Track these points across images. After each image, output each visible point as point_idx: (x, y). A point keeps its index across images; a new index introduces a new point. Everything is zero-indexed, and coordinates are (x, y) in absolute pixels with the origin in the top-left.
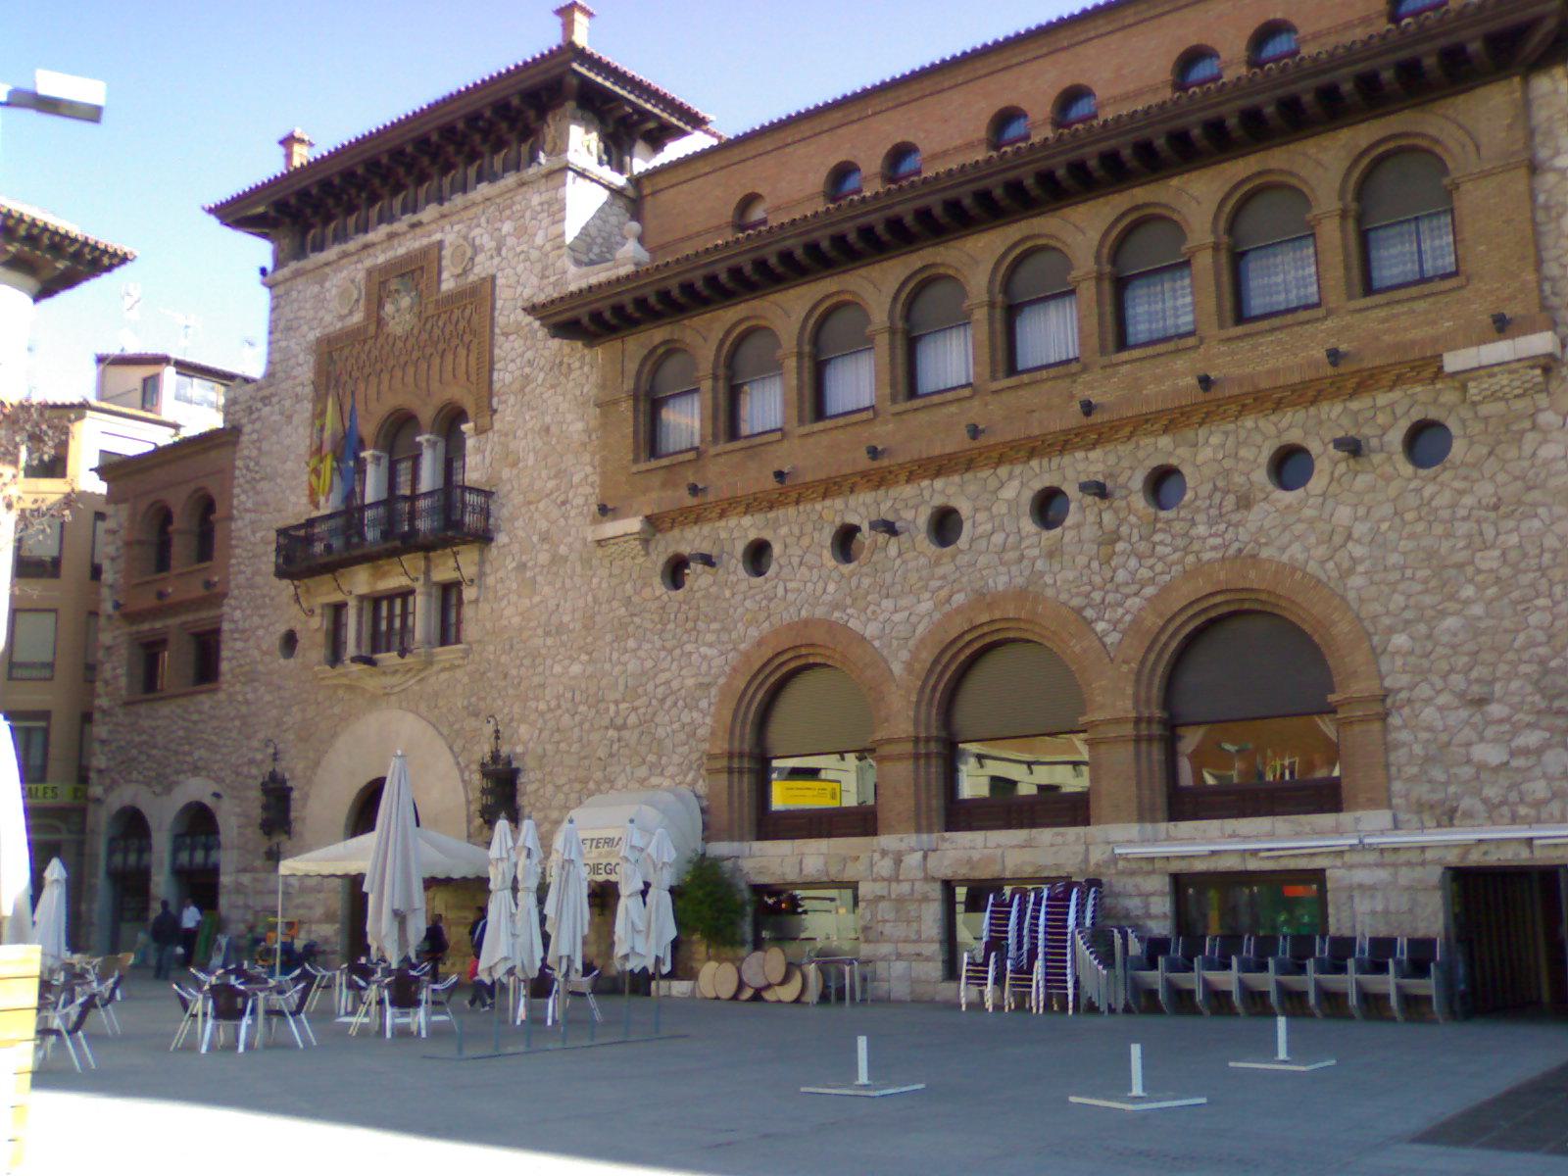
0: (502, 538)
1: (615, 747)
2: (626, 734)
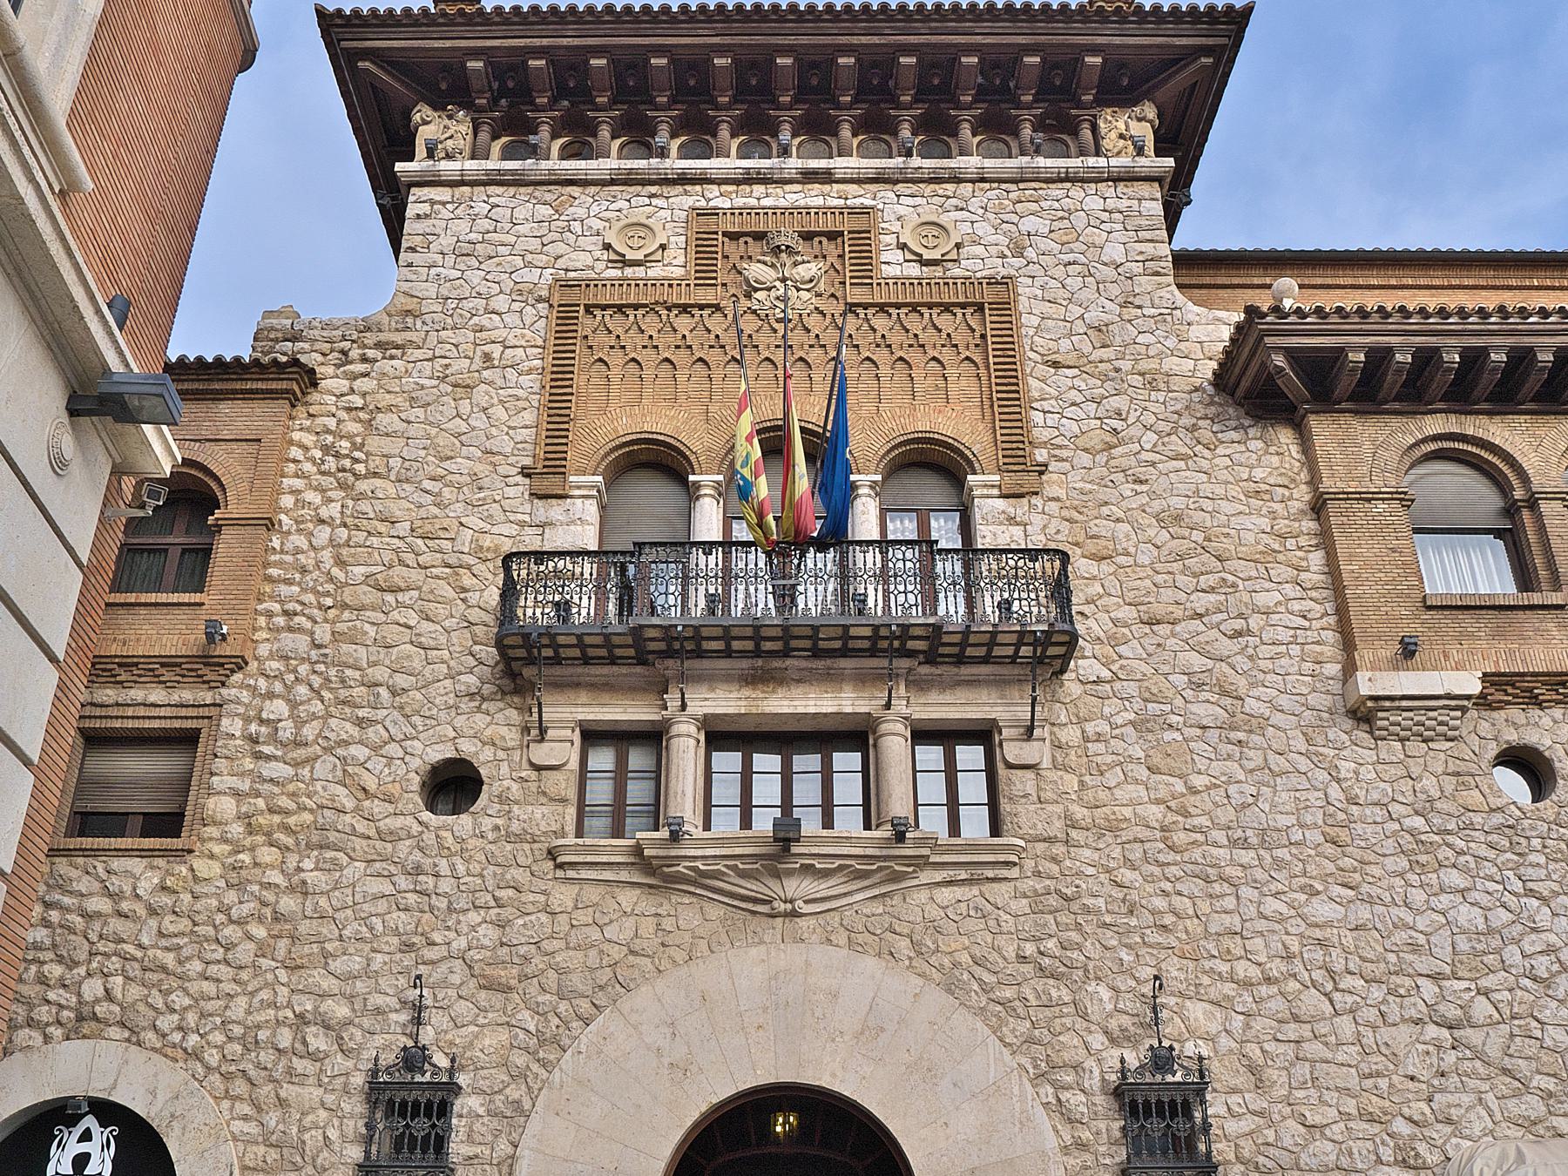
0: (1085, 666)
2: (1473, 1036)
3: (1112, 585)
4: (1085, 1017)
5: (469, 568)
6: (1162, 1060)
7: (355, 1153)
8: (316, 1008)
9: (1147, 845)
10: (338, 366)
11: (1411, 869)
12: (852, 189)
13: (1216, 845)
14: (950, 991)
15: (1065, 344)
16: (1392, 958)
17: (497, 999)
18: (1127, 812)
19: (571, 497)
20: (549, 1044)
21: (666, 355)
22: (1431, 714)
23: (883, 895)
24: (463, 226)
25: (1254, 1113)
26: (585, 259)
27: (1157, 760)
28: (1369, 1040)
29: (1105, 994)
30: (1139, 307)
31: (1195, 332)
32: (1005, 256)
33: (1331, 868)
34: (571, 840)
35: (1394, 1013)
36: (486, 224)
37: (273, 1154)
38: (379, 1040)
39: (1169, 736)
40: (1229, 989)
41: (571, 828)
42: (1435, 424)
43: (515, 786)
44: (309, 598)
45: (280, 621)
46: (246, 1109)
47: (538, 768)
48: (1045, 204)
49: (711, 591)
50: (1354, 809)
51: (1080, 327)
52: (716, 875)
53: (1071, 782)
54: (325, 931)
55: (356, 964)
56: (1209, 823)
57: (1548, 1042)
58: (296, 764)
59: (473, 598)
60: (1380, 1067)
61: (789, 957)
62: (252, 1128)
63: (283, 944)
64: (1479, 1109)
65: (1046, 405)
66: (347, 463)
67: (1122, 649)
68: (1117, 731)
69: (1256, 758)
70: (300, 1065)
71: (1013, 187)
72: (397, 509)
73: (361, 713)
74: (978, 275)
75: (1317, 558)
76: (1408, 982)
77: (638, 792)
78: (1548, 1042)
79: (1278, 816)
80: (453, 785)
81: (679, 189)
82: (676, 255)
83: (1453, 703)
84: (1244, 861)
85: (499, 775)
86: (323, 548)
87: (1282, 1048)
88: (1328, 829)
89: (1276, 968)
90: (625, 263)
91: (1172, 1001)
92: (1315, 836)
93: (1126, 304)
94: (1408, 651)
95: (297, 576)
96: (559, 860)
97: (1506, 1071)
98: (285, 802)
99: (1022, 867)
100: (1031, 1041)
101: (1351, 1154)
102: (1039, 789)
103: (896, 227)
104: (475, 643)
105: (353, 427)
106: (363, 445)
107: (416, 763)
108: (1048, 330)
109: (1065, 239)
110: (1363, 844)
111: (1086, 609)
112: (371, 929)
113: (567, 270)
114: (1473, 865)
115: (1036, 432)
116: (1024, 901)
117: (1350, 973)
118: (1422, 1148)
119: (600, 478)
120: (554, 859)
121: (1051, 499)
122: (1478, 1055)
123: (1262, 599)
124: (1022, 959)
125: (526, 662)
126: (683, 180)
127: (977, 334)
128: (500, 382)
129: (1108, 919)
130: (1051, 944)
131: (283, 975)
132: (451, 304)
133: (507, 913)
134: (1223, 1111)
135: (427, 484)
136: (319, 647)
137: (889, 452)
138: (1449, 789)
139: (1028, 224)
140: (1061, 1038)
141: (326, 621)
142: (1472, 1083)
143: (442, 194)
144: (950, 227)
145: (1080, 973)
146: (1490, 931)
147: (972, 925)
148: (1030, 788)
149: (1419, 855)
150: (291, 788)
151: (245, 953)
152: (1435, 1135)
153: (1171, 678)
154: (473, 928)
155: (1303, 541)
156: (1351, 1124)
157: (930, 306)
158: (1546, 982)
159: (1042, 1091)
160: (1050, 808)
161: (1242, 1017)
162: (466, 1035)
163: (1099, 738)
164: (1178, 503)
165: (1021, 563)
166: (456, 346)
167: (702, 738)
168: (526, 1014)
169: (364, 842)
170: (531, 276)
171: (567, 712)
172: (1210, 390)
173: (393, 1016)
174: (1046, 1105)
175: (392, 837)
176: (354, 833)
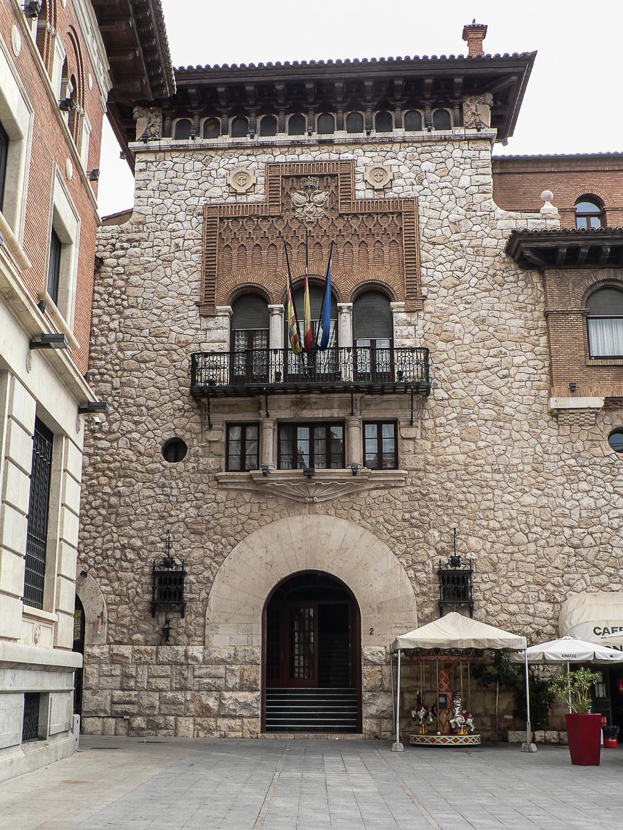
0: (440, 393)
1: (573, 560)
2: (583, 551)
3: (452, 353)
4: (428, 543)
5: (175, 350)
6: (455, 561)
7: (148, 597)
8: (129, 542)
9: (458, 472)
10: (111, 252)
11: (567, 482)
12: (343, 148)
13: (486, 472)
14: (374, 533)
15: (439, 232)
16: (554, 519)
17: (198, 538)
18: (450, 458)
19: (218, 316)
20: (220, 555)
21: (257, 242)
22: (582, 415)
23: (350, 494)
24: (162, 174)
25: (492, 581)
26: (218, 193)
27: (465, 435)
28: (541, 552)
29: (436, 534)
30: (475, 211)
31: (500, 224)
32: (413, 185)
33: (533, 481)
34: (224, 473)
35: (552, 540)
36: (171, 174)
37: (118, 599)
38: (154, 554)
39: (471, 424)
40: (486, 532)
41: (223, 467)
42: (602, 275)
43: (200, 450)
44: (109, 366)
45: (98, 377)
46: (106, 582)
47: (210, 442)
48: (434, 154)
49: (278, 371)
50: (546, 456)
51: (446, 223)
52: (283, 487)
53: (428, 445)
54: (129, 511)
55: (142, 524)
56: (484, 463)
57: (614, 554)
58: (111, 441)
59: (178, 364)
60: (544, 563)
61: (311, 520)
62: (108, 588)
63: (113, 516)
64: (582, 580)
65: (428, 265)
66: (119, 301)
67: (454, 385)
68: (449, 422)
69: (506, 433)
70: (125, 564)
71: (419, 145)
72: (143, 323)
73: (136, 418)
74: (400, 195)
75: (543, 340)
76: (559, 529)
77: (250, 449)
78: (614, 554)
79: (513, 459)
80: (174, 449)
81: (261, 151)
82: (260, 188)
83: (591, 411)
84: (497, 479)
85: (195, 446)
86: (113, 343)
87: (505, 556)
88: (534, 465)
89: (506, 523)
90: (236, 193)
91: (463, 537)
92: (528, 468)
93: (468, 210)
94: (573, 390)
95: (103, 356)
96: (219, 481)
97: (595, 566)
98: (108, 458)
99: (406, 481)
100: (406, 552)
101: (528, 597)
102: (415, 448)
103: (362, 169)
104: (181, 386)
105: (120, 283)
106: (125, 291)
107: (159, 440)
108: (431, 225)
109: (443, 174)
110: (548, 471)
111: (440, 366)
112: (147, 510)
113: (210, 198)
114: (593, 480)
115: (423, 279)
116: (406, 496)
117: (537, 526)
118: (557, 595)
119: (230, 307)
120: (218, 480)
121: (428, 313)
122: (585, 559)
123: (517, 360)
124: (405, 520)
125: (203, 397)
126: (263, 146)
127: (398, 228)
128: (183, 258)
129: (440, 503)
130: (416, 514)
131: (114, 529)
132: (159, 218)
133: (200, 503)
134: (479, 580)
135: (155, 311)
136: (116, 389)
137: (357, 289)
138: (587, 447)
139: (426, 166)
140: (418, 552)
141: (117, 377)
142: (580, 570)
143: (151, 157)
144: (387, 169)
145: (427, 525)
146: (597, 508)
147: (384, 506)
148: (411, 448)
149: (572, 476)
150: (110, 451)
151: (99, 520)
152: (563, 590)
153: (474, 397)
154: (187, 509)
155: (538, 331)
156: (530, 586)
157: (377, 214)
158: (617, 530)
159: (409, 572)
160: (419, 456)
161: (490, 544)
162: (187, 551)
163: (441, 425)
164: (484, 313)
165: (407, 354)
166: (163, 240)
167: (276, 427)
168: (209, 544)
169: (141, 474)
170: (193, 201)
171: (219, 418)
172: (504, 255)
173: (159, 545)
174: (410, 578)
175: (152, 472)
176: (137, 470)
